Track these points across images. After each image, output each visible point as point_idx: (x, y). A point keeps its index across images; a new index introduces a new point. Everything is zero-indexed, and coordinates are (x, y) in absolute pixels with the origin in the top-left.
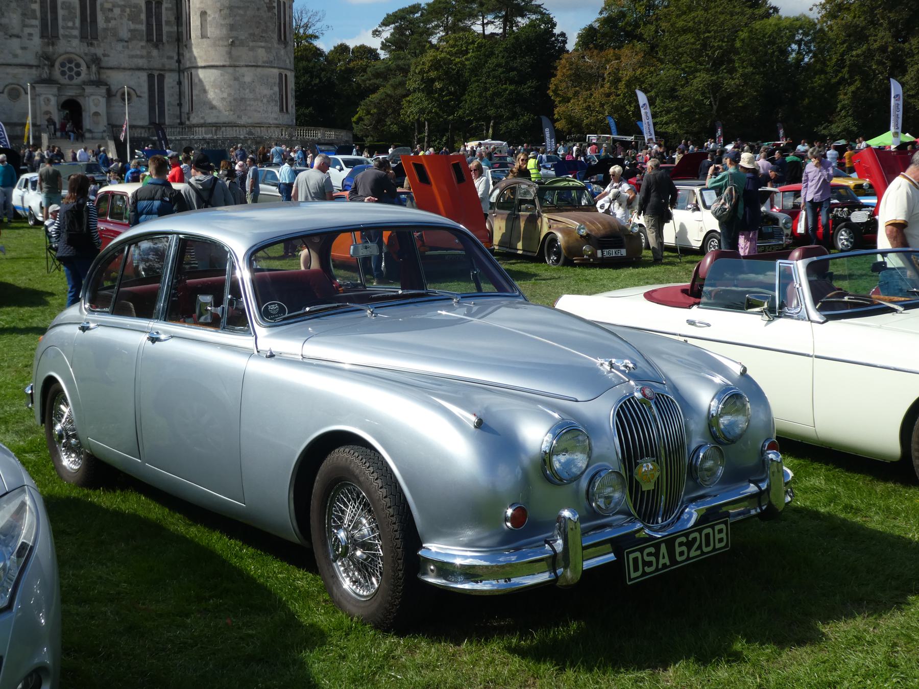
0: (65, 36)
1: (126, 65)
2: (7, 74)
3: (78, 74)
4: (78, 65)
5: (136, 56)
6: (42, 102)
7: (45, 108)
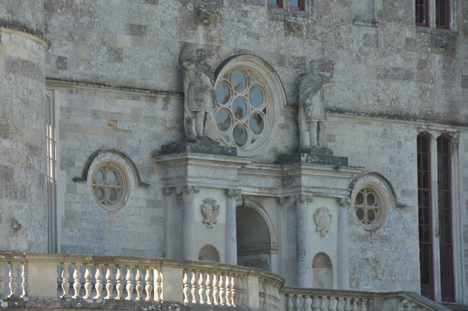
2: (95, 115)
6: (198, 217)
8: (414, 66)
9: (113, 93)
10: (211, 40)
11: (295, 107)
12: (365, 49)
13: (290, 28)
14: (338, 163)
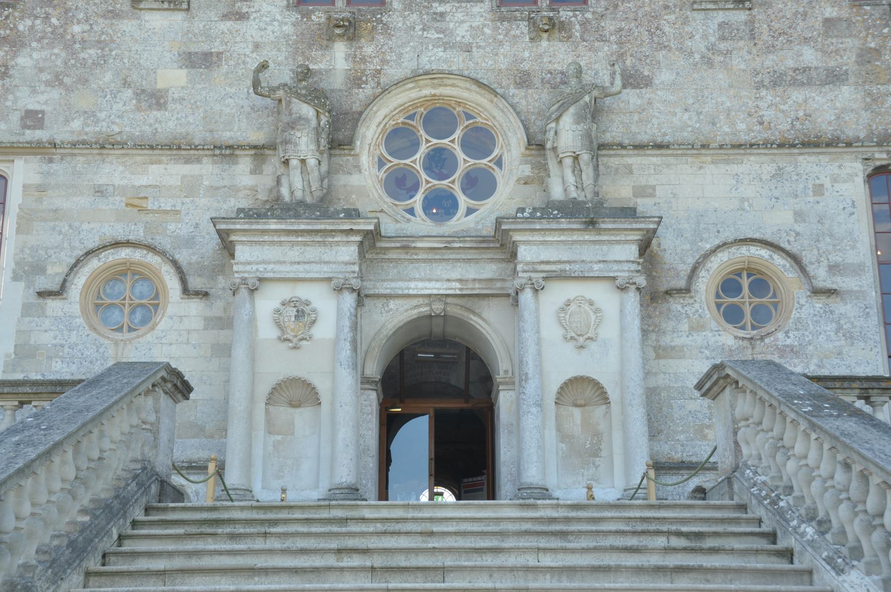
1: (743, 130)
2: (100, 191)
3: (479, 185)
4: (480, 141)
5: (803, 77)
6: (267, 331)
7: (279, 364)
8: (849, 61)
9: (140, 157)
10: (363, 60)
12: (722, 46)
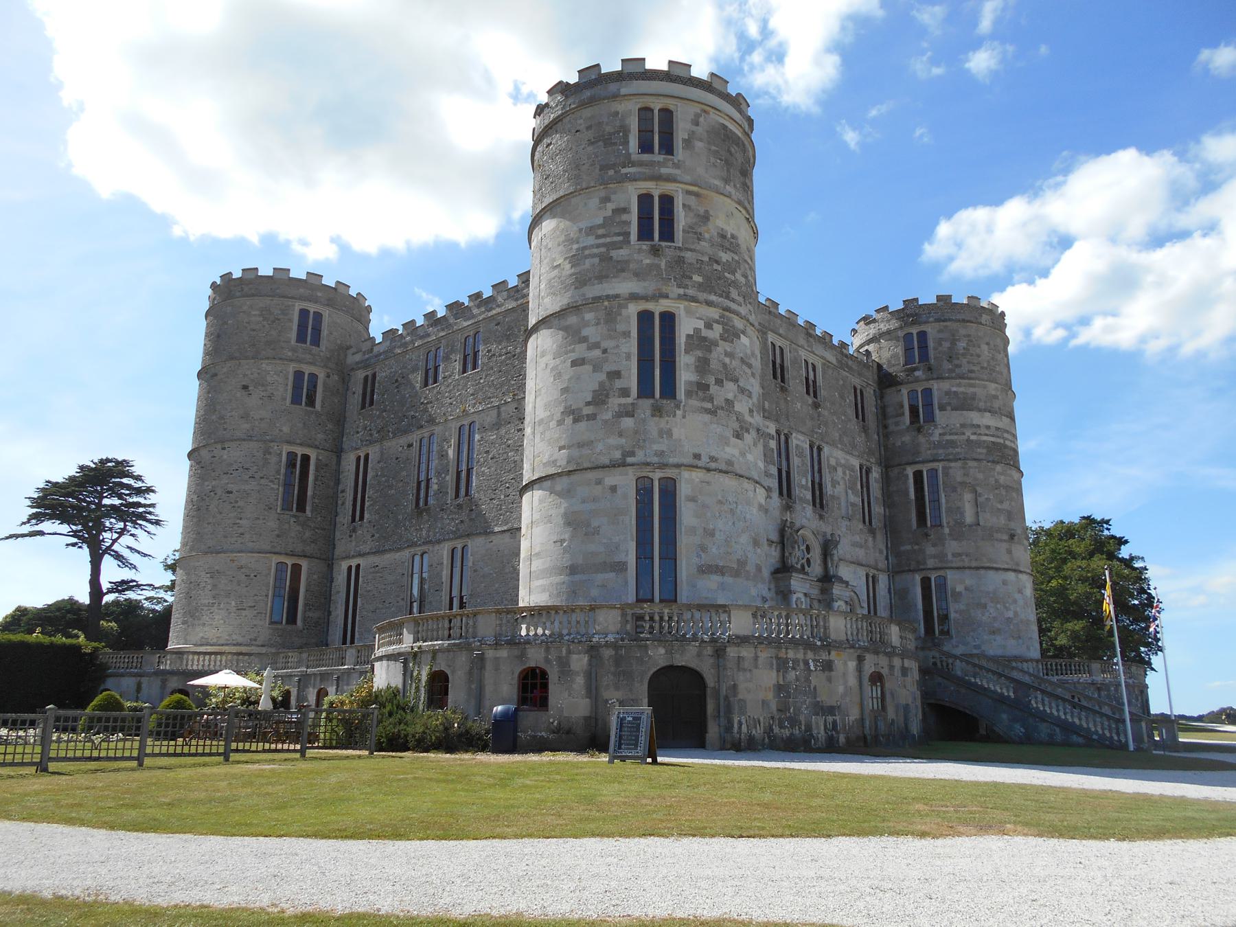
0: (801, 499)
11: (826, 553)
13: (821, 517)
14: (847, 583)
